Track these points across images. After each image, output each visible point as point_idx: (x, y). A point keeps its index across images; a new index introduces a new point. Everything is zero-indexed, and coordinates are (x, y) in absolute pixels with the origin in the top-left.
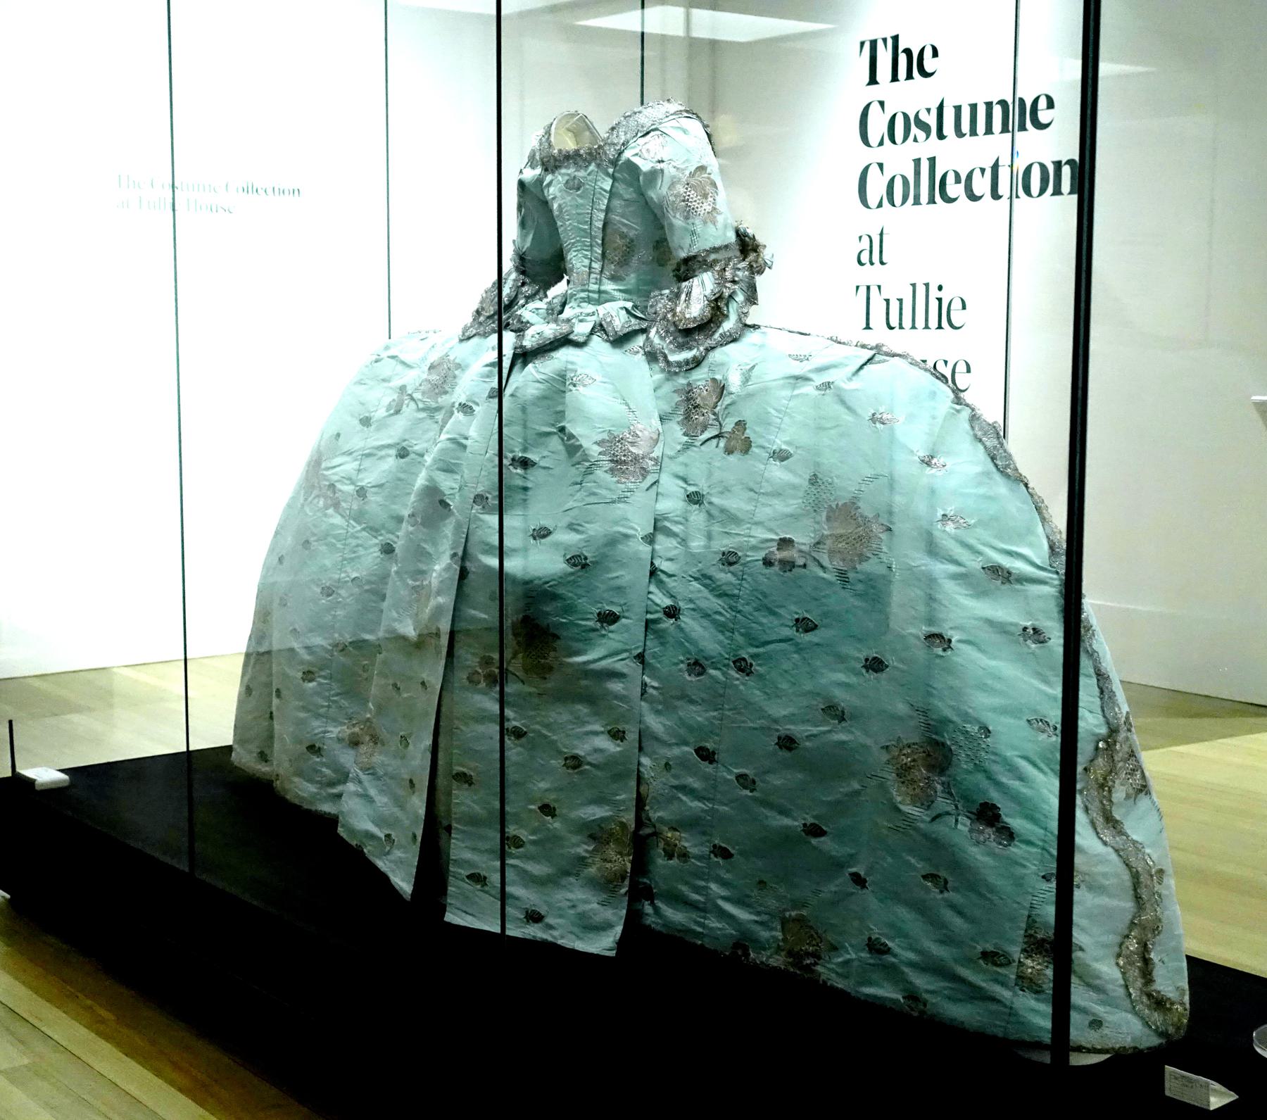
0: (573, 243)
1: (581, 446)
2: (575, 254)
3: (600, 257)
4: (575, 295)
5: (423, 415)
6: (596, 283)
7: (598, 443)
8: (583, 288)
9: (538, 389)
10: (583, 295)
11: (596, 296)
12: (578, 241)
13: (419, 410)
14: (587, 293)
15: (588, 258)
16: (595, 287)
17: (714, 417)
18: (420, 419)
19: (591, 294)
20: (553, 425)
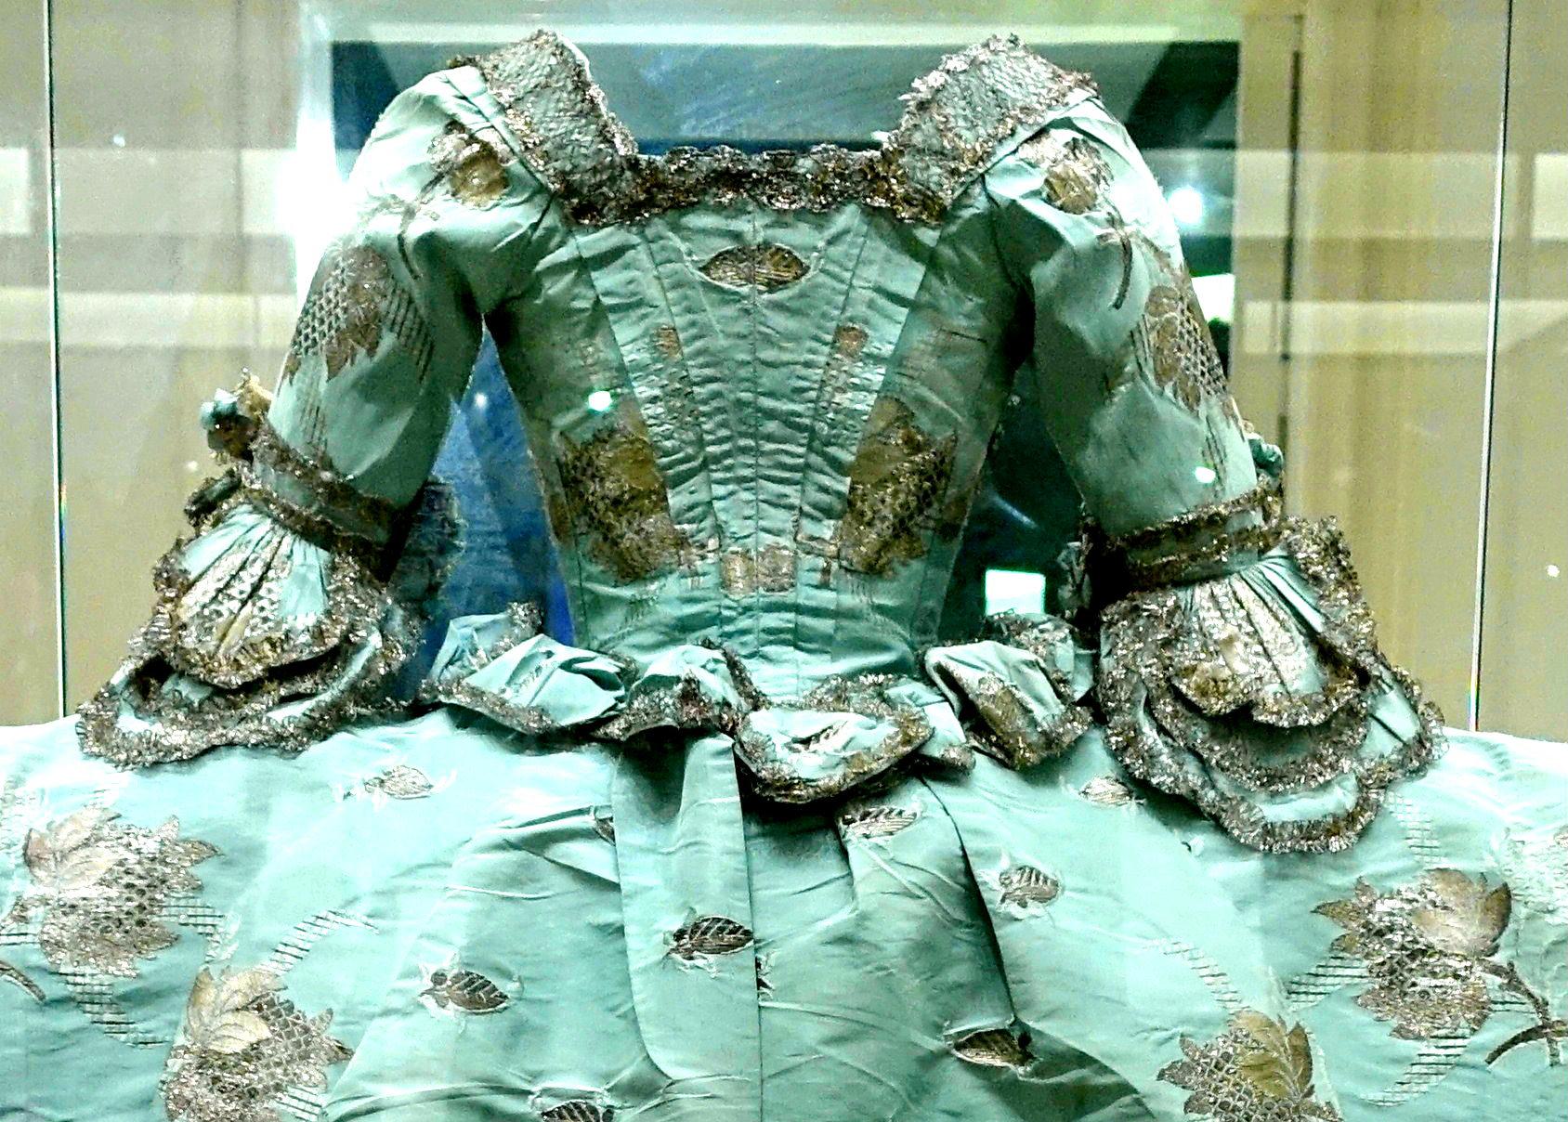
0: (717, 459)
1: (1125, 1089)
2: (720, 490)
3: (838, 506)
4: (730, 620)
5: (71, 1020)
6: (824, 585)
7: (1172, 1074)
8: (777, 597)
9: (910, 916)
10: (771, 620)
11: (826, 625)
12: (744, 450)
13: (46, 1004)
14: (791, 616)
15: (791, 507)
16: (826, 598)
17: (1498, 980)
18: (64, 1036)
19: (808, 621)
20: (939, 1028)
